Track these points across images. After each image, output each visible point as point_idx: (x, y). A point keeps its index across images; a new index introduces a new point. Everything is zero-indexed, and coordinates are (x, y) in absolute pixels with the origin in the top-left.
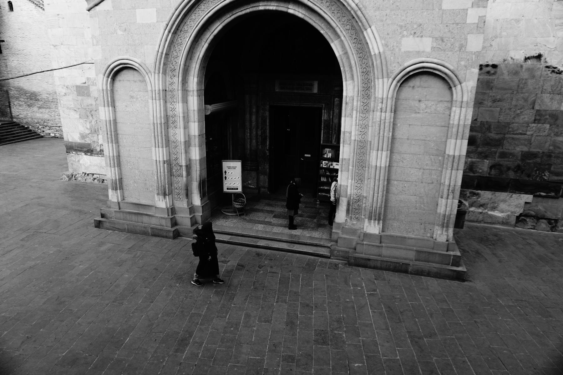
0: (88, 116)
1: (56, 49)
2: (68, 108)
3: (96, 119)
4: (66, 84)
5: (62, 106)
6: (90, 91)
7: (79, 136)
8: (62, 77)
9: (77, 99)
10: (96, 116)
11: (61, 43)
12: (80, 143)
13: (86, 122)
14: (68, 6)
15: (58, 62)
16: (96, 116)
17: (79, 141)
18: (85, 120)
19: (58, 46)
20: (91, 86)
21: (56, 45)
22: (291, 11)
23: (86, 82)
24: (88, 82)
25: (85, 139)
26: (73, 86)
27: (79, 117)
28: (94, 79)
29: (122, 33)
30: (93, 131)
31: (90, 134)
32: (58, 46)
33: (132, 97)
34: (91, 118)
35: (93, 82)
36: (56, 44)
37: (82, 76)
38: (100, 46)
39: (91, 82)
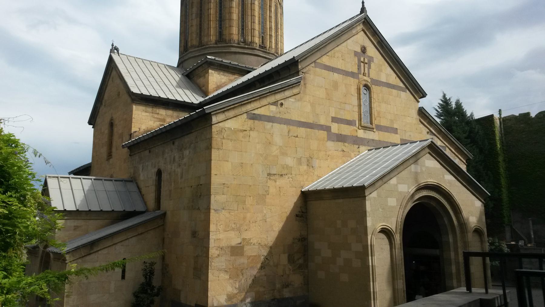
0: (238, 275)
1: (217, 213)
2: (219, 270)
3: (246, 277)
4: (221, 246)
5: (213, 268)
6: (244, 250)
7: (226, 298)
8: (218, 239)
9: (229, 259)
10: (247, 274)
11: (223, 208)
12: (227, 305)
13: (236, 281)
14: (234, 178)
15: (217, 224)
16: (247, 274)
17: (225, 303)
18: (234, 280)
19: (220, 210)
20: (245, 246)
21: (217, 210)
22: (432, 203)
23: (241, 243)
24: (243, 243)
25: (232, 300)
26: (228, 247)
27: (229, 277)
28: (249, 239)
29: (381, 210)
30: (241, 290)
31: (238, 294)
32: (220, 210)
33: (382, 249)
34: (241, 277)
35: (248, 242)
36: (217, 209)
37: (238, 237)
38: (371, 218)
39: (246, 242)
